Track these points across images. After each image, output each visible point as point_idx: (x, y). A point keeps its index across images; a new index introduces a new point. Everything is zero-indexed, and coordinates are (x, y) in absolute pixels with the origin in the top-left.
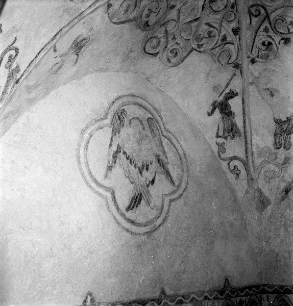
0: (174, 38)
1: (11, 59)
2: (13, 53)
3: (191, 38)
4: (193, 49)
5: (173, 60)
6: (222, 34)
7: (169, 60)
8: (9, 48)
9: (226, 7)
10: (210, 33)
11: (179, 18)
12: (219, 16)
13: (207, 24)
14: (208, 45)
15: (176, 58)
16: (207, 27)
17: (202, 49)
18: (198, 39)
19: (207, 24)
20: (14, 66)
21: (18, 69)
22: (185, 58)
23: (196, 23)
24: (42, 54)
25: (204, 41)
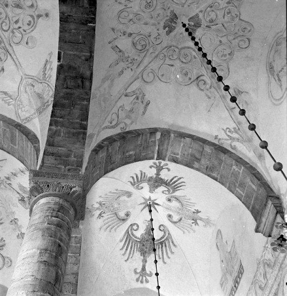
0: (236, 33)
1: (230, 132)
2: (228, 130)
3: (233, 24)
4: (240, 19)
5: (249, 29)
6: (227, 5)
7: (249, 31)
8: (225, 132)
9: (213, 11)
10: (228, 13)
11: (225, 35)
12: (218, 13)
13: (224, 18)
14: (235, 11)
15: (247, 27)
16: (226, 17)
17: (238, 14)
18: (233, 19)
19: (224, 18)
20: (233, 130)
21: (234, 128)
22: (246, 22)
23: (225, 25)
24: (233, 116)
25: (233, 14)
